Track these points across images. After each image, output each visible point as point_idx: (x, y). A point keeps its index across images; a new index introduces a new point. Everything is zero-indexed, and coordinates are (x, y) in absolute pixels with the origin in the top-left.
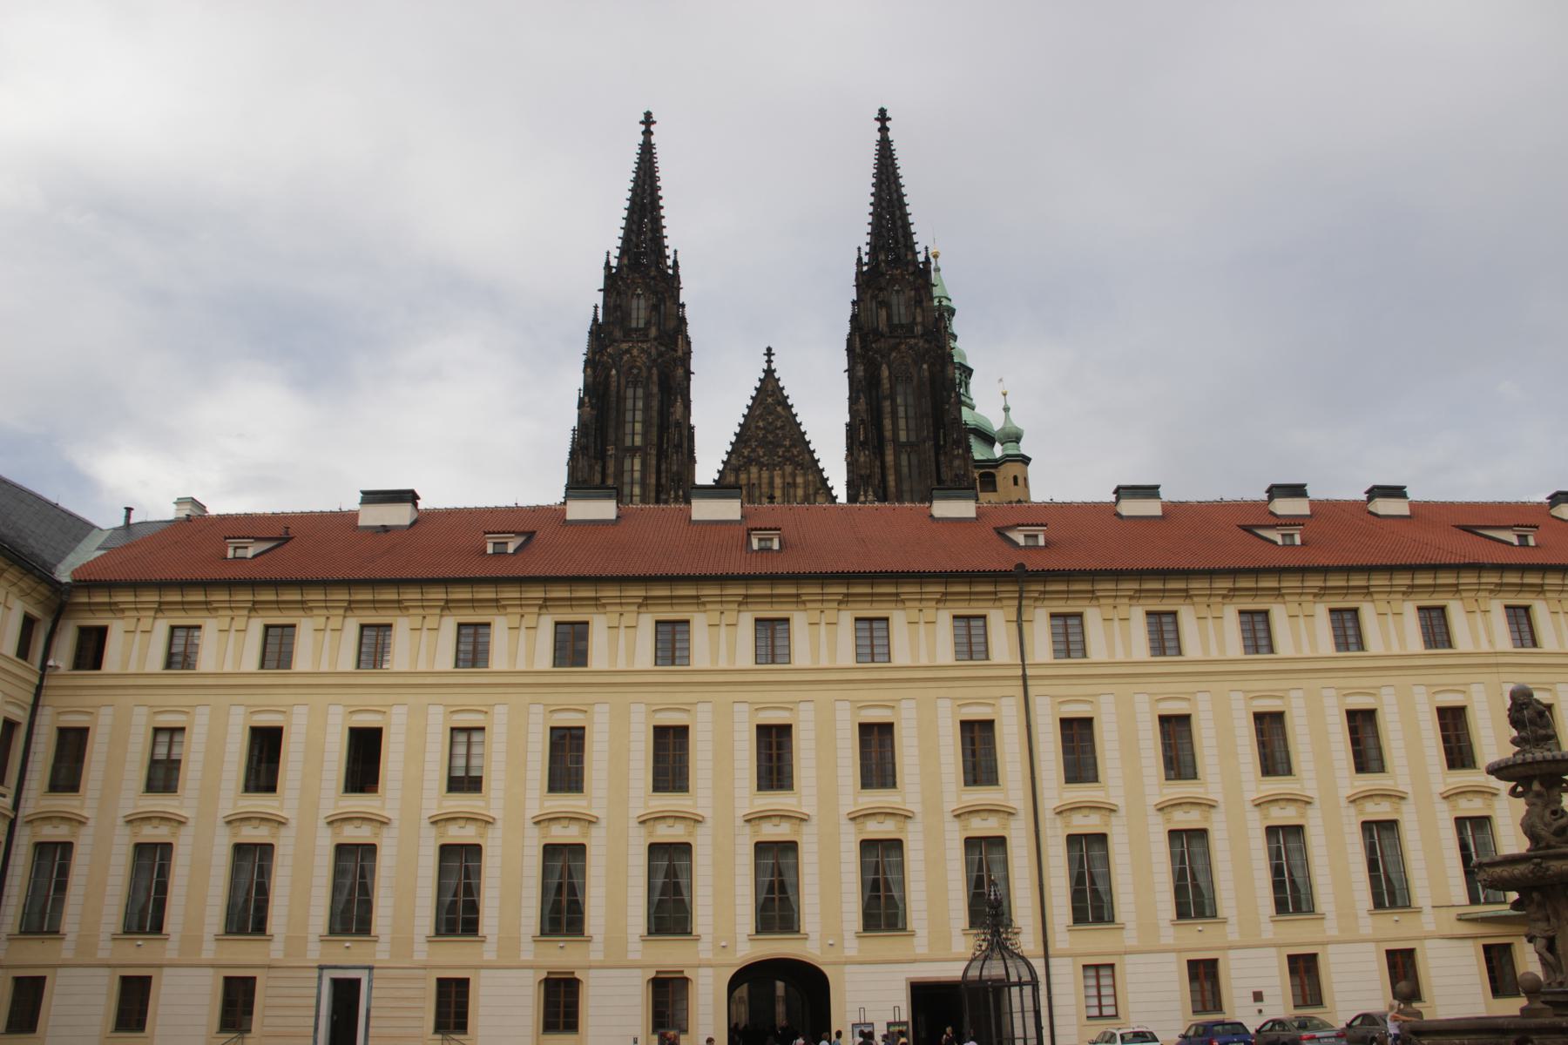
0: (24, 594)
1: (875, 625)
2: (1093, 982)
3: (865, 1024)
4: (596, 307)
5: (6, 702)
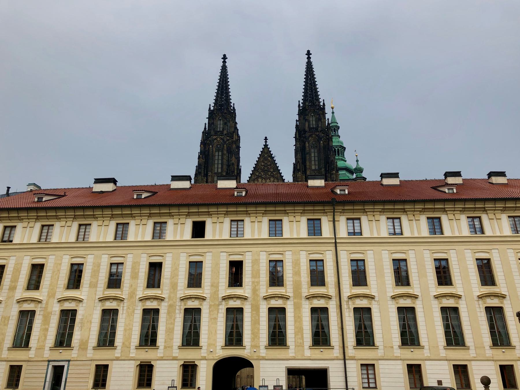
2: (365, 372)
3: (264, 386)
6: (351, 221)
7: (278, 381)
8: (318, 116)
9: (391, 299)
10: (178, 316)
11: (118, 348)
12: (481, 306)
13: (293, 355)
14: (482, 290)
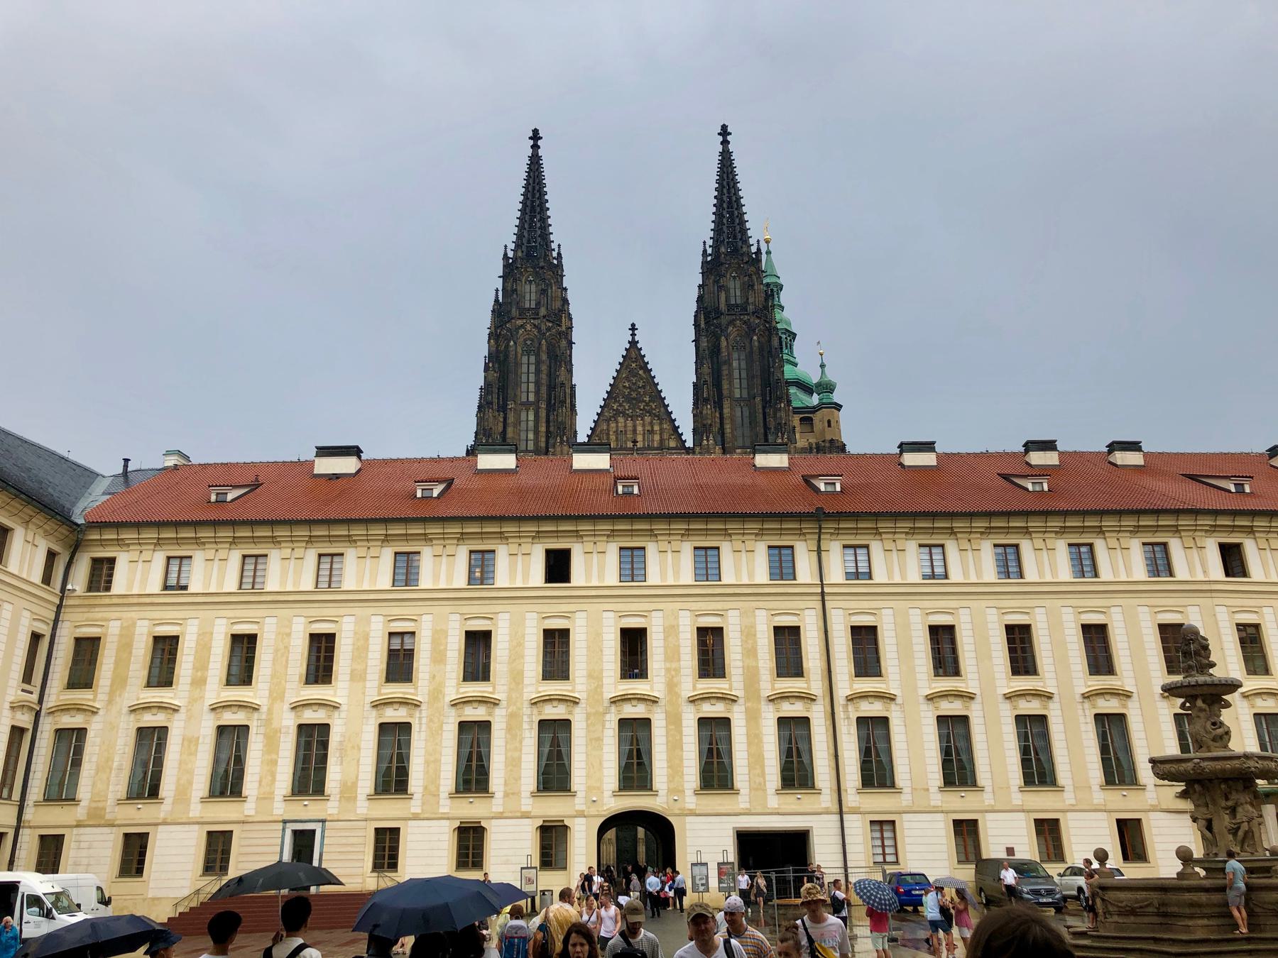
0: (47, 534)
1: (709, 552)
2: (878, 835)
4: (497, 290)
5: (34, 619)
6: (851, 551)
9: (927, 702)
10: (527, 734)
11: (415, 797)
12: (1087, 712)
13: (747, 805)
14: (1090, 683)
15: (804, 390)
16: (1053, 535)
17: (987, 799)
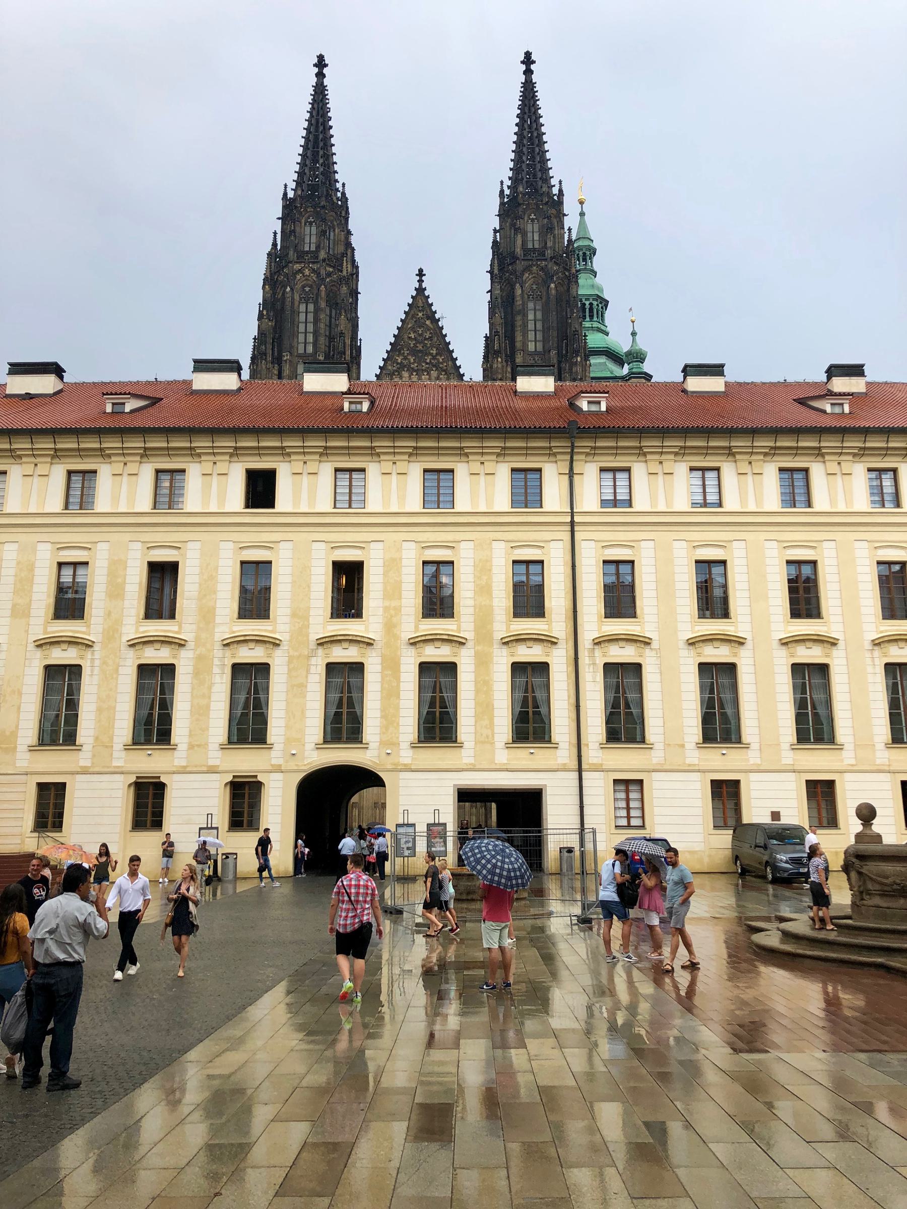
1: (442, 476)
2: (622, 795)
3: (408, 824)
4: (275, 233)
6: (610, 475)
7: (437, 815)
8: (546, 221)
9: (686, 647)
10: (217, 679)
11: (84, 748)
12: (877, 661)
13: (472, 760)
14: (882, 628)
15: (615, 360)
16: (850, 458)
17: (752, 757)
